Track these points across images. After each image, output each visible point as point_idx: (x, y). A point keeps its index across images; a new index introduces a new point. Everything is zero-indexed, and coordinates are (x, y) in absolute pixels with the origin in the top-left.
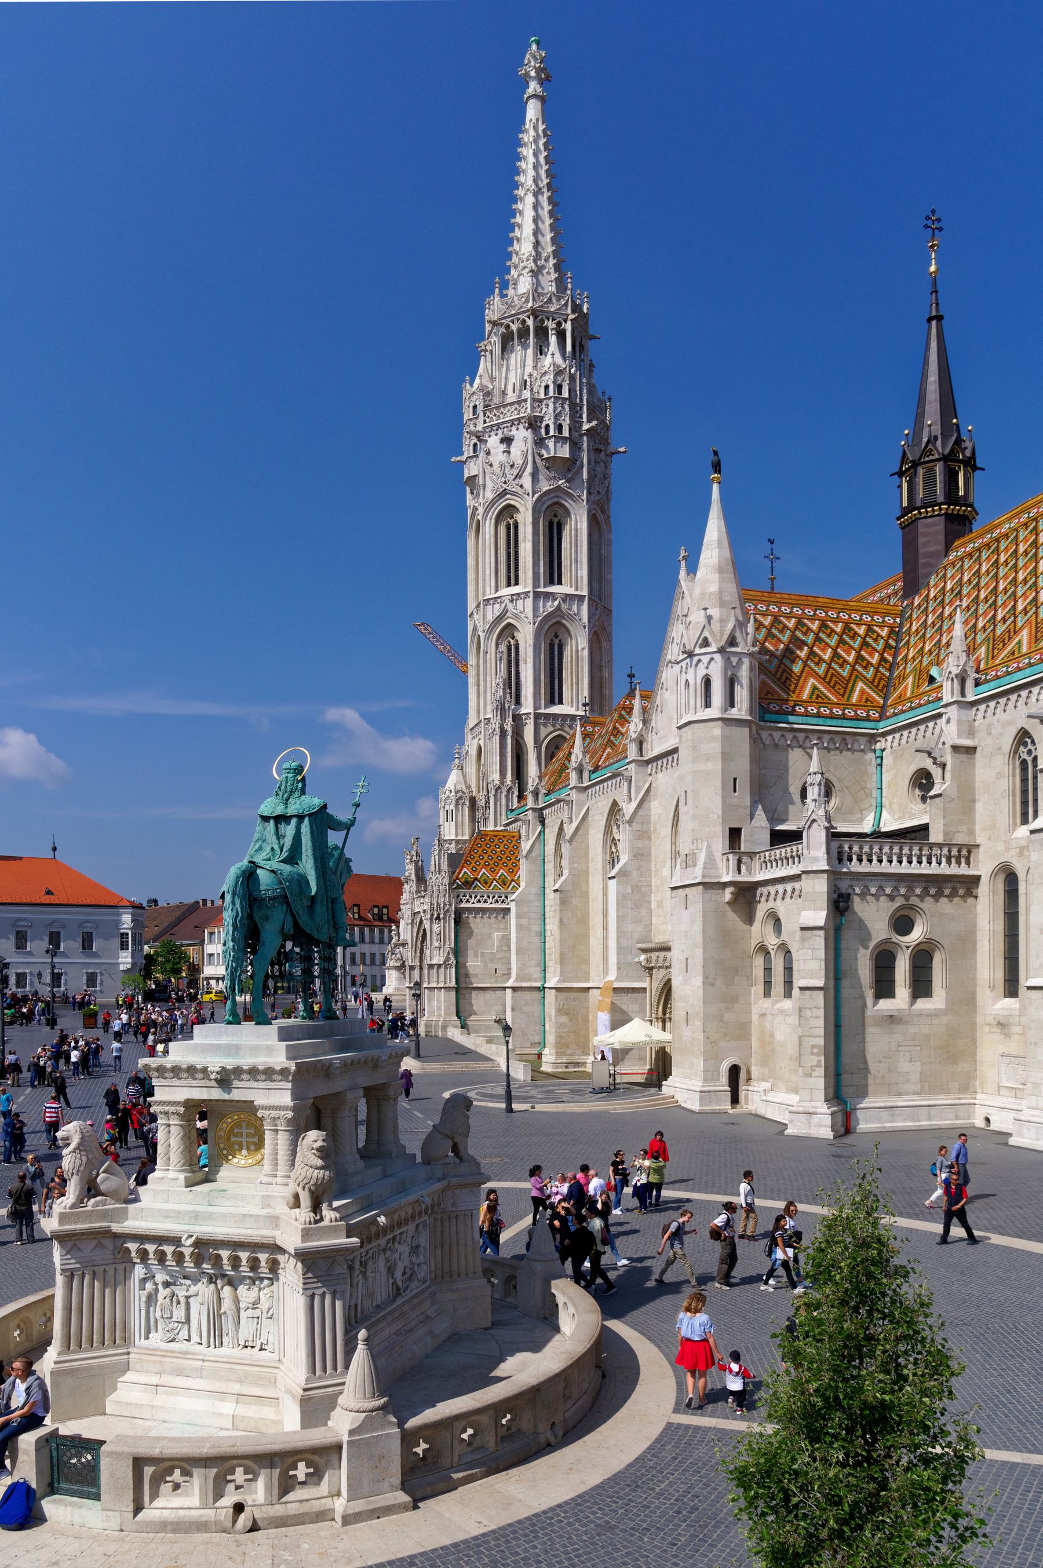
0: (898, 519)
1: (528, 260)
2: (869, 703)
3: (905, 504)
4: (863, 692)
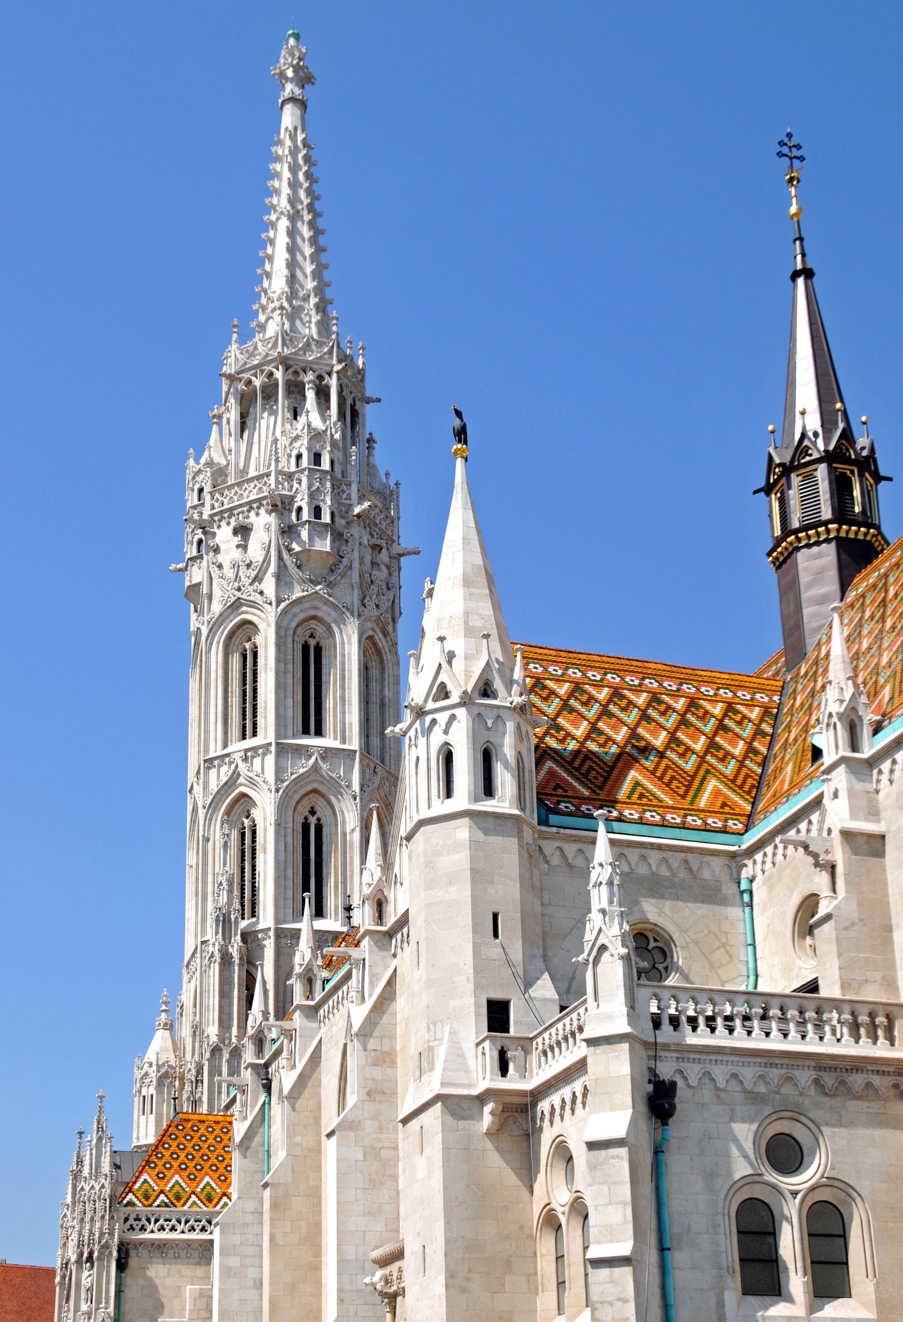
0: (769, 554)
1: (279, 299)
2: (727, 809)
3: (778, 532)
4: (717, 793)
